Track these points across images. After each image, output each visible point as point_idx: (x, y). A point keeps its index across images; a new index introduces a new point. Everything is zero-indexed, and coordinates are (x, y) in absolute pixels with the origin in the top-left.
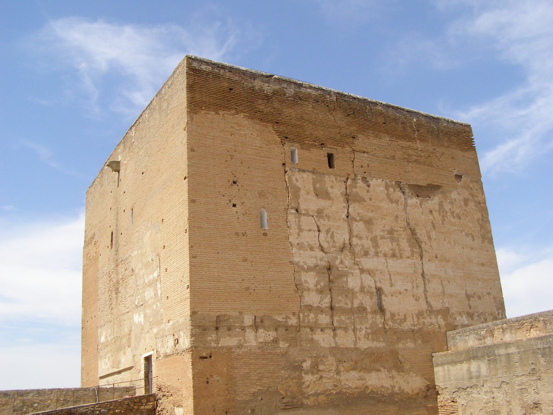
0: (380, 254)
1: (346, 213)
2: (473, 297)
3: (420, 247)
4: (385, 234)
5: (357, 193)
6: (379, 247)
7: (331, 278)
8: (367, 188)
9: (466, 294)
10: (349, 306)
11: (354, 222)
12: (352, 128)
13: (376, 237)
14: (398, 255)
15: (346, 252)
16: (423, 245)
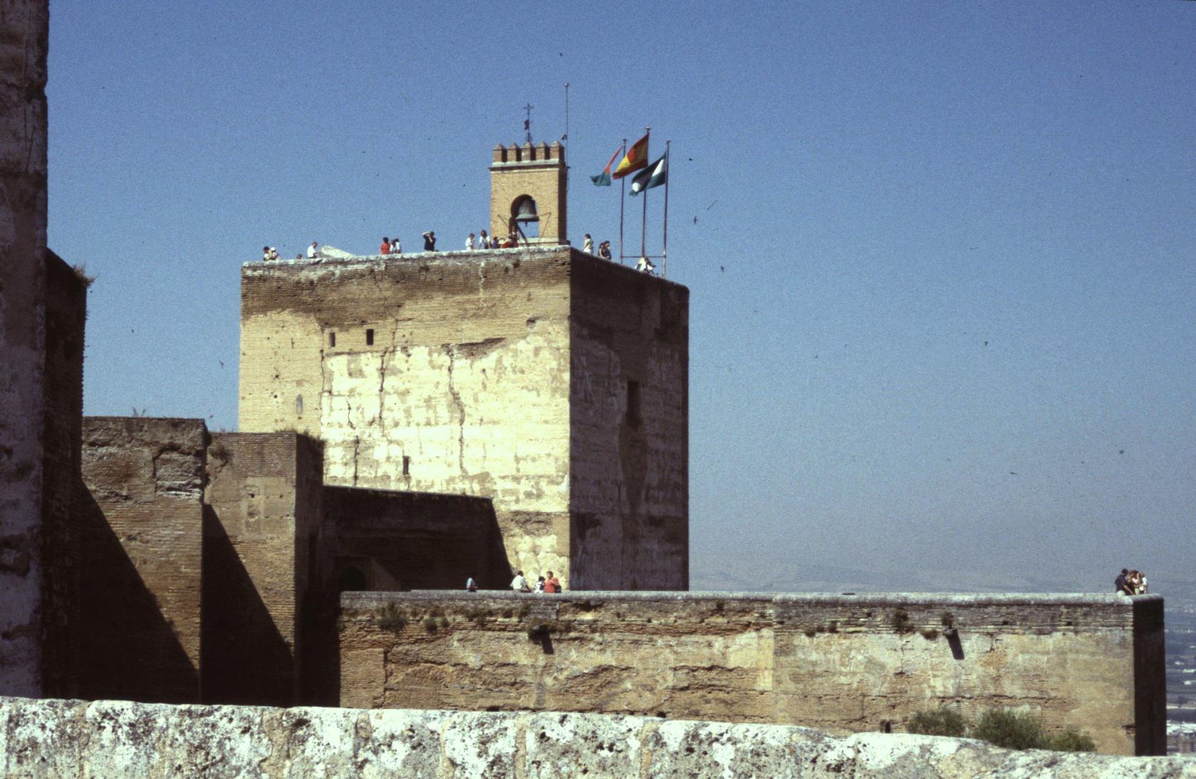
0: (412, 424)
1: (379, 388)
2: (525, 459)
3: (462, 411)
4: (422, 403)
5: (394, 366)
6: (411, 417)
7: (358, 451)
8: (406, 358)
9: (516, 456)
10: (373, 475)
11: (387, 397)
12: (401, 295)
13: (410, 407)
14: (433, 422)
15: (375, 425)
16: (467, 410)
